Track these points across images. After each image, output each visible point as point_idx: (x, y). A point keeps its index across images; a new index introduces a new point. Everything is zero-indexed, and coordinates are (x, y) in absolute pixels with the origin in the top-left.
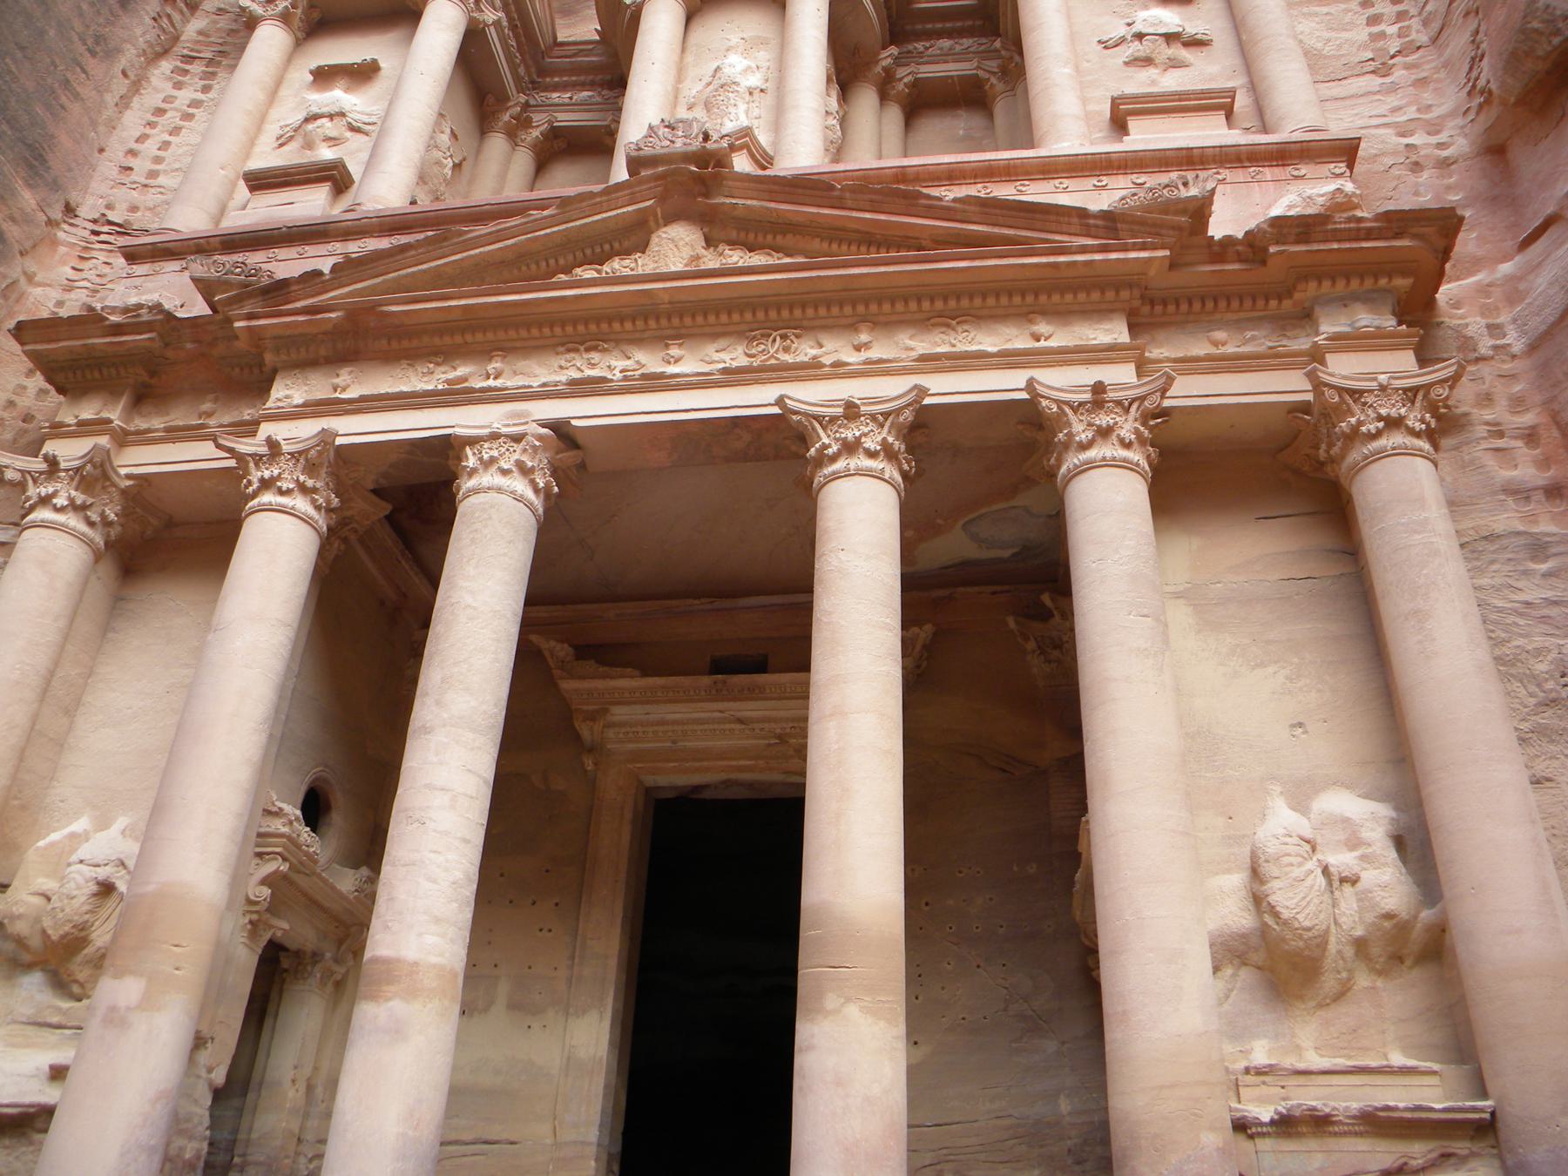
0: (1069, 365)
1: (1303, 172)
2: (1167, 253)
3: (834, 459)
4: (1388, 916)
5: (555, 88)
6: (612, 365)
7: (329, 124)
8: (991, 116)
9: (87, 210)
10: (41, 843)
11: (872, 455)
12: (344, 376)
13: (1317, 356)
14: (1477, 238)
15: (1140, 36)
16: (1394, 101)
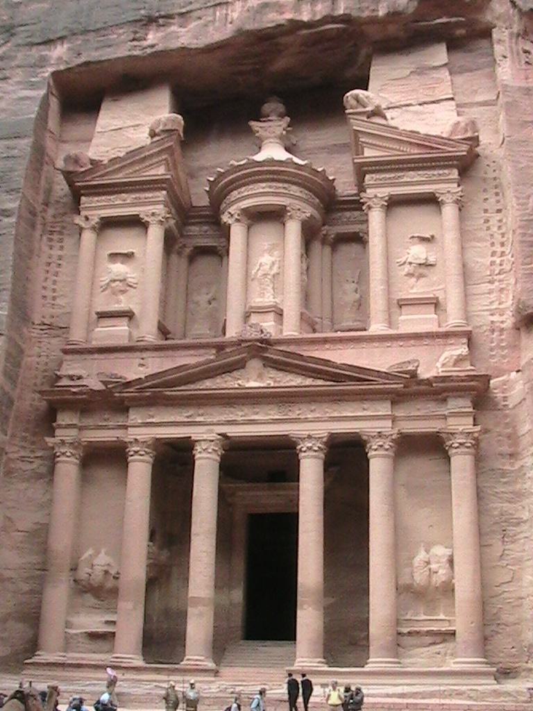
0: (372, 422)
1: (452, 342)
2: (402, 385)
3: (305, 452)
4: (443, 582)
5: (193, 224)
6: (238, 414)
7: (121, 284)
8: (365, 248)
9: (36, 322)
10: (83, 558)
11: (316, 451)
12: (153, 411)
13: (445, 417)
14: (508, 362)
15: (410, 263)
16: (493, 296)
